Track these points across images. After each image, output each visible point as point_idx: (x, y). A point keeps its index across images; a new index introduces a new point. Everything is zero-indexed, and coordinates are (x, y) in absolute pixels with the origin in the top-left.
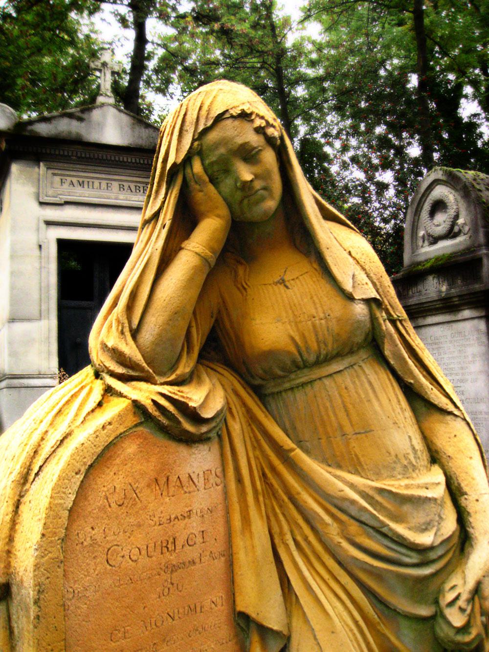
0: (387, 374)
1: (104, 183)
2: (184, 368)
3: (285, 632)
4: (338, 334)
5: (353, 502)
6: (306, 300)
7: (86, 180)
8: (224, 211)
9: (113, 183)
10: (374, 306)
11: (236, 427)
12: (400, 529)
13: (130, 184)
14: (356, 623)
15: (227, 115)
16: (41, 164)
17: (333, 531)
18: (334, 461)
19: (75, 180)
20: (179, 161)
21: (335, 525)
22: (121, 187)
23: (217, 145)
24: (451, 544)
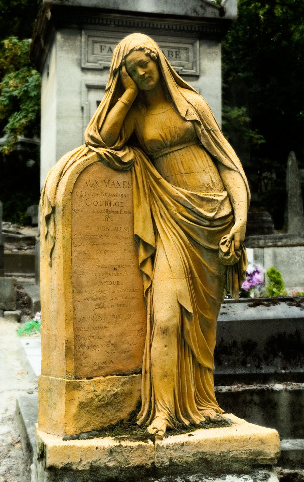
0: (204, 153)
3: (154, 246)
4: (179, 134)
5: (181, 198)
6: (167, 121)
8: (134, 86)
10: (196, 124)
11: (138, 168)
12: (201, 210)
14: (181, 244)
15: (135, 49)
16: (83, 32)
17: (173, 209)
20: (117, 67)
21: (175, 207)
23: (130, 61)
24: (227, 221)
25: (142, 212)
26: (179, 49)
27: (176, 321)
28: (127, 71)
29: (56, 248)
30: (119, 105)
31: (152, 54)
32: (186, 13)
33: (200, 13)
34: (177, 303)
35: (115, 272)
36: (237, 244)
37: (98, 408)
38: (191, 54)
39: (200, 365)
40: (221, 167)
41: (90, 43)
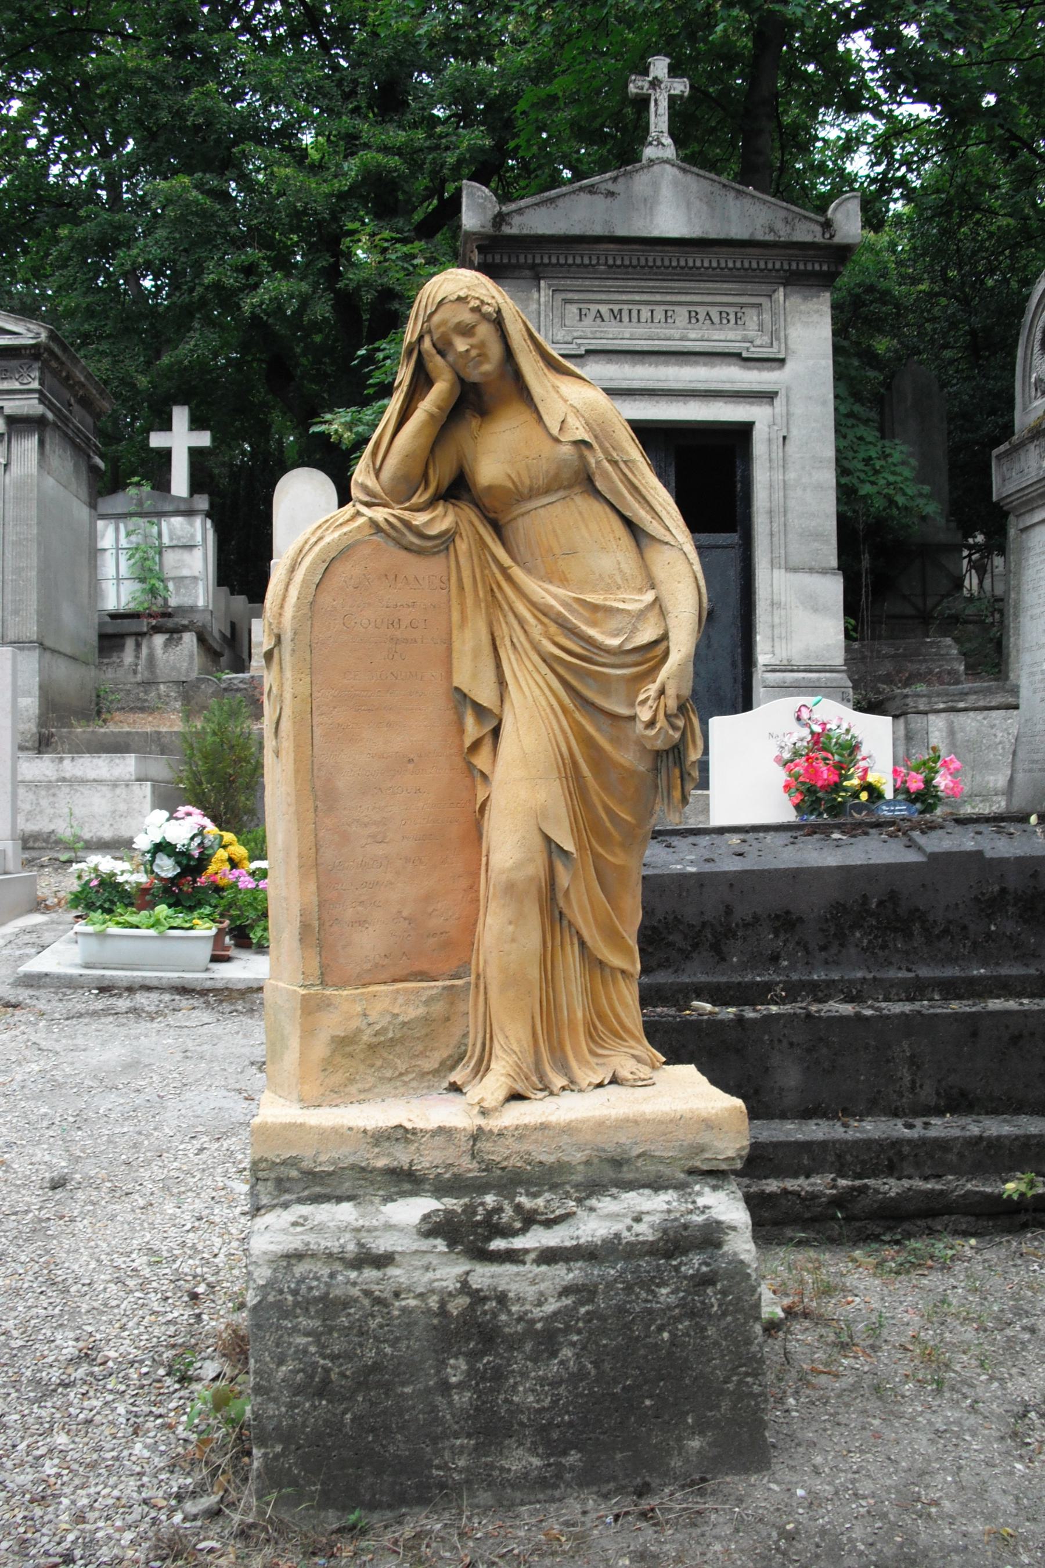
3: (496, 711)
5: (552, 607)
7: (625, 307)
9: (676, 308)
10: (583, 447)
12: (592, 632)
13: (709, 308)
14: (551, 706)
16: (542, 283)
17: (536, 630)
19: (604, 309)
20: (414, 339)
22: (693, 317)
25: (469, 641)
26: (742, 306)
27: (537, 868)
28: (434, 345)
29: (284, 719)
30: (418, 417)
31: (486, 309)
32: (752, 234)
33: (782, 233)
34: (537, 832)
35: (411, 766)
36: (672, 704)
37: (372, 1047)
38: (766, 317)
39: (601, 962)
40: (644, 541)
41: (558, 303)
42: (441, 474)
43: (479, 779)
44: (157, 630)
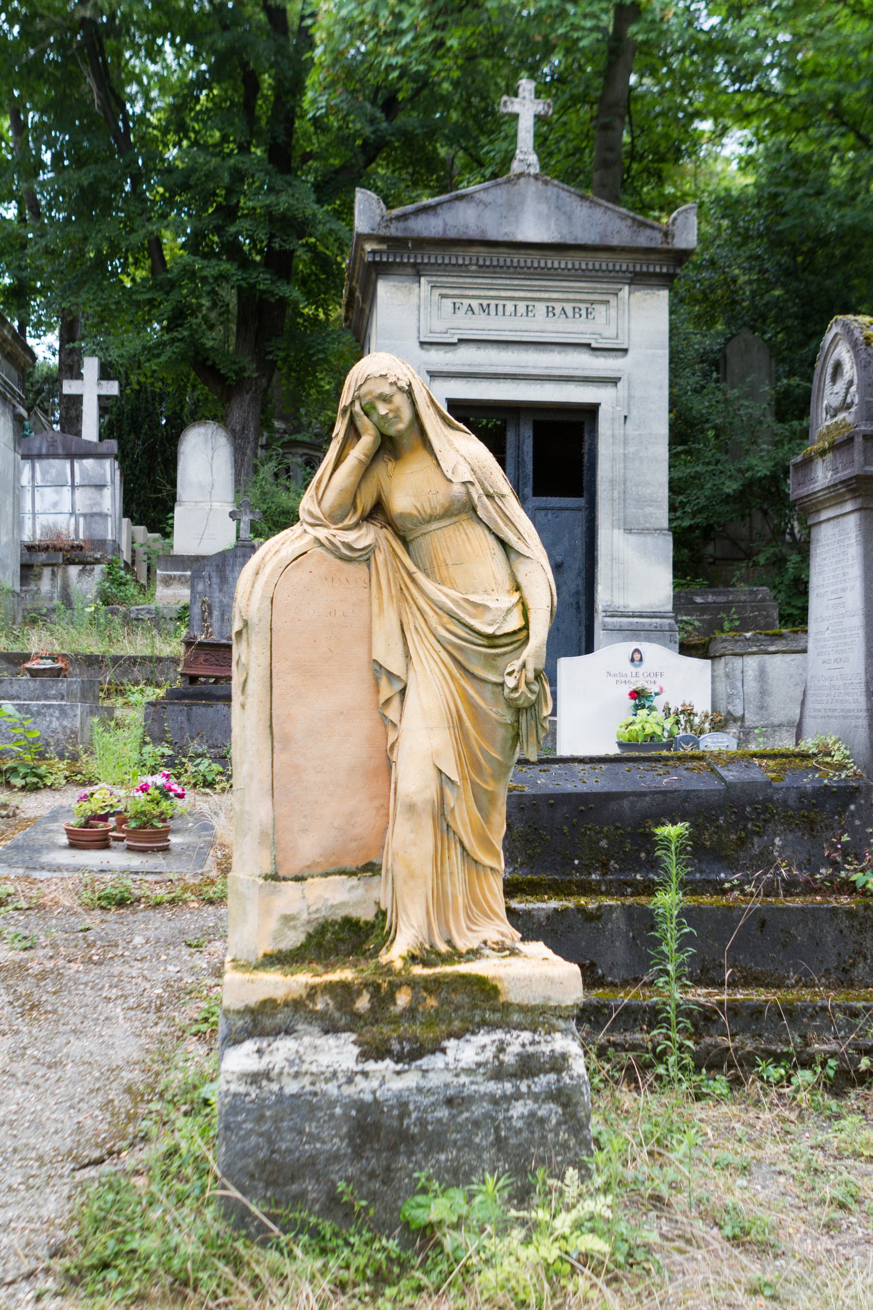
1: (521, 306)
2: (348, 522)
3: (403, 677)
7: (493, 303)
9: (537, 304)
11: (380, 557)
18: (442, 582)
19: (475, 303)
23: (365, 395)
25: (386, 626)
26: (593, 302)
27: (432, 792)
29: (250, 681)
31: (400, 384)
34: (432, 767)
36: (531, 675)
38: (613, 312)
40: (513, 556)
42: (366, 501)
43: (390, 727)
44: (70, 562)
